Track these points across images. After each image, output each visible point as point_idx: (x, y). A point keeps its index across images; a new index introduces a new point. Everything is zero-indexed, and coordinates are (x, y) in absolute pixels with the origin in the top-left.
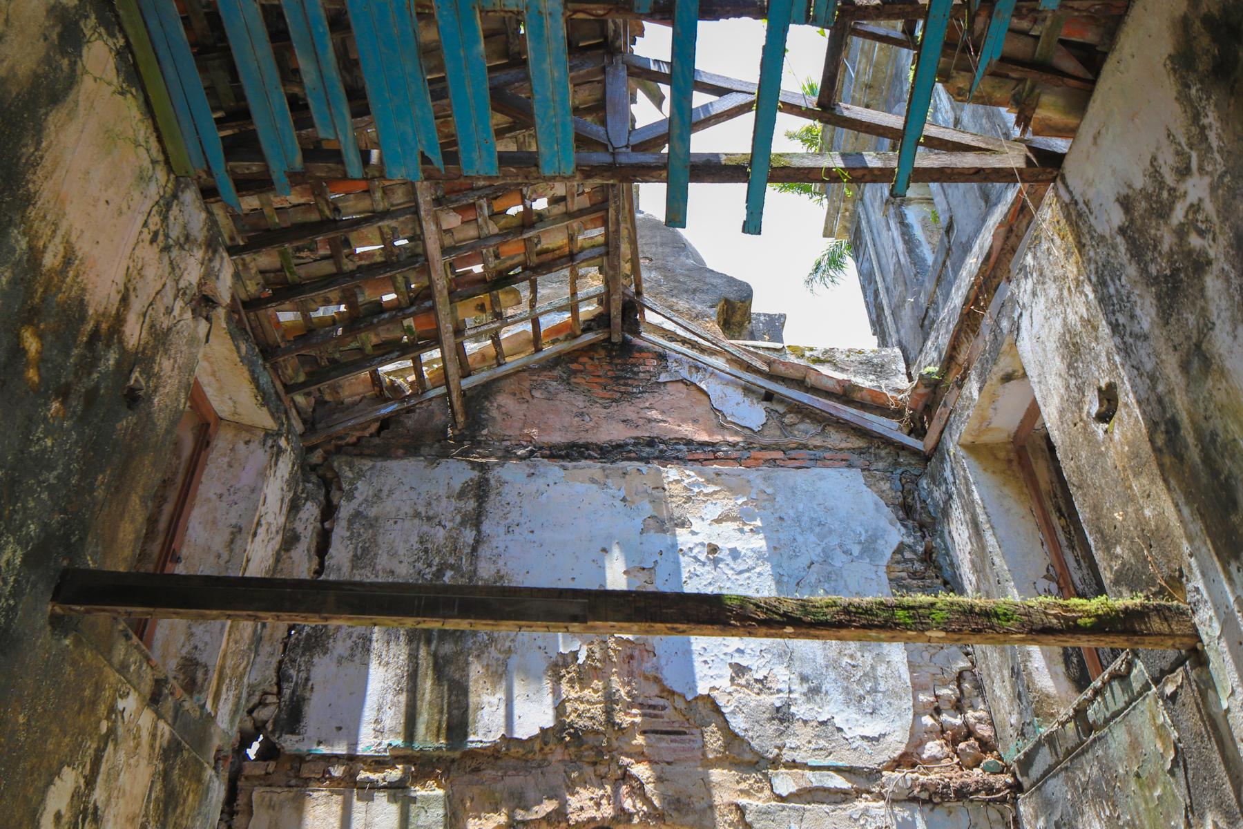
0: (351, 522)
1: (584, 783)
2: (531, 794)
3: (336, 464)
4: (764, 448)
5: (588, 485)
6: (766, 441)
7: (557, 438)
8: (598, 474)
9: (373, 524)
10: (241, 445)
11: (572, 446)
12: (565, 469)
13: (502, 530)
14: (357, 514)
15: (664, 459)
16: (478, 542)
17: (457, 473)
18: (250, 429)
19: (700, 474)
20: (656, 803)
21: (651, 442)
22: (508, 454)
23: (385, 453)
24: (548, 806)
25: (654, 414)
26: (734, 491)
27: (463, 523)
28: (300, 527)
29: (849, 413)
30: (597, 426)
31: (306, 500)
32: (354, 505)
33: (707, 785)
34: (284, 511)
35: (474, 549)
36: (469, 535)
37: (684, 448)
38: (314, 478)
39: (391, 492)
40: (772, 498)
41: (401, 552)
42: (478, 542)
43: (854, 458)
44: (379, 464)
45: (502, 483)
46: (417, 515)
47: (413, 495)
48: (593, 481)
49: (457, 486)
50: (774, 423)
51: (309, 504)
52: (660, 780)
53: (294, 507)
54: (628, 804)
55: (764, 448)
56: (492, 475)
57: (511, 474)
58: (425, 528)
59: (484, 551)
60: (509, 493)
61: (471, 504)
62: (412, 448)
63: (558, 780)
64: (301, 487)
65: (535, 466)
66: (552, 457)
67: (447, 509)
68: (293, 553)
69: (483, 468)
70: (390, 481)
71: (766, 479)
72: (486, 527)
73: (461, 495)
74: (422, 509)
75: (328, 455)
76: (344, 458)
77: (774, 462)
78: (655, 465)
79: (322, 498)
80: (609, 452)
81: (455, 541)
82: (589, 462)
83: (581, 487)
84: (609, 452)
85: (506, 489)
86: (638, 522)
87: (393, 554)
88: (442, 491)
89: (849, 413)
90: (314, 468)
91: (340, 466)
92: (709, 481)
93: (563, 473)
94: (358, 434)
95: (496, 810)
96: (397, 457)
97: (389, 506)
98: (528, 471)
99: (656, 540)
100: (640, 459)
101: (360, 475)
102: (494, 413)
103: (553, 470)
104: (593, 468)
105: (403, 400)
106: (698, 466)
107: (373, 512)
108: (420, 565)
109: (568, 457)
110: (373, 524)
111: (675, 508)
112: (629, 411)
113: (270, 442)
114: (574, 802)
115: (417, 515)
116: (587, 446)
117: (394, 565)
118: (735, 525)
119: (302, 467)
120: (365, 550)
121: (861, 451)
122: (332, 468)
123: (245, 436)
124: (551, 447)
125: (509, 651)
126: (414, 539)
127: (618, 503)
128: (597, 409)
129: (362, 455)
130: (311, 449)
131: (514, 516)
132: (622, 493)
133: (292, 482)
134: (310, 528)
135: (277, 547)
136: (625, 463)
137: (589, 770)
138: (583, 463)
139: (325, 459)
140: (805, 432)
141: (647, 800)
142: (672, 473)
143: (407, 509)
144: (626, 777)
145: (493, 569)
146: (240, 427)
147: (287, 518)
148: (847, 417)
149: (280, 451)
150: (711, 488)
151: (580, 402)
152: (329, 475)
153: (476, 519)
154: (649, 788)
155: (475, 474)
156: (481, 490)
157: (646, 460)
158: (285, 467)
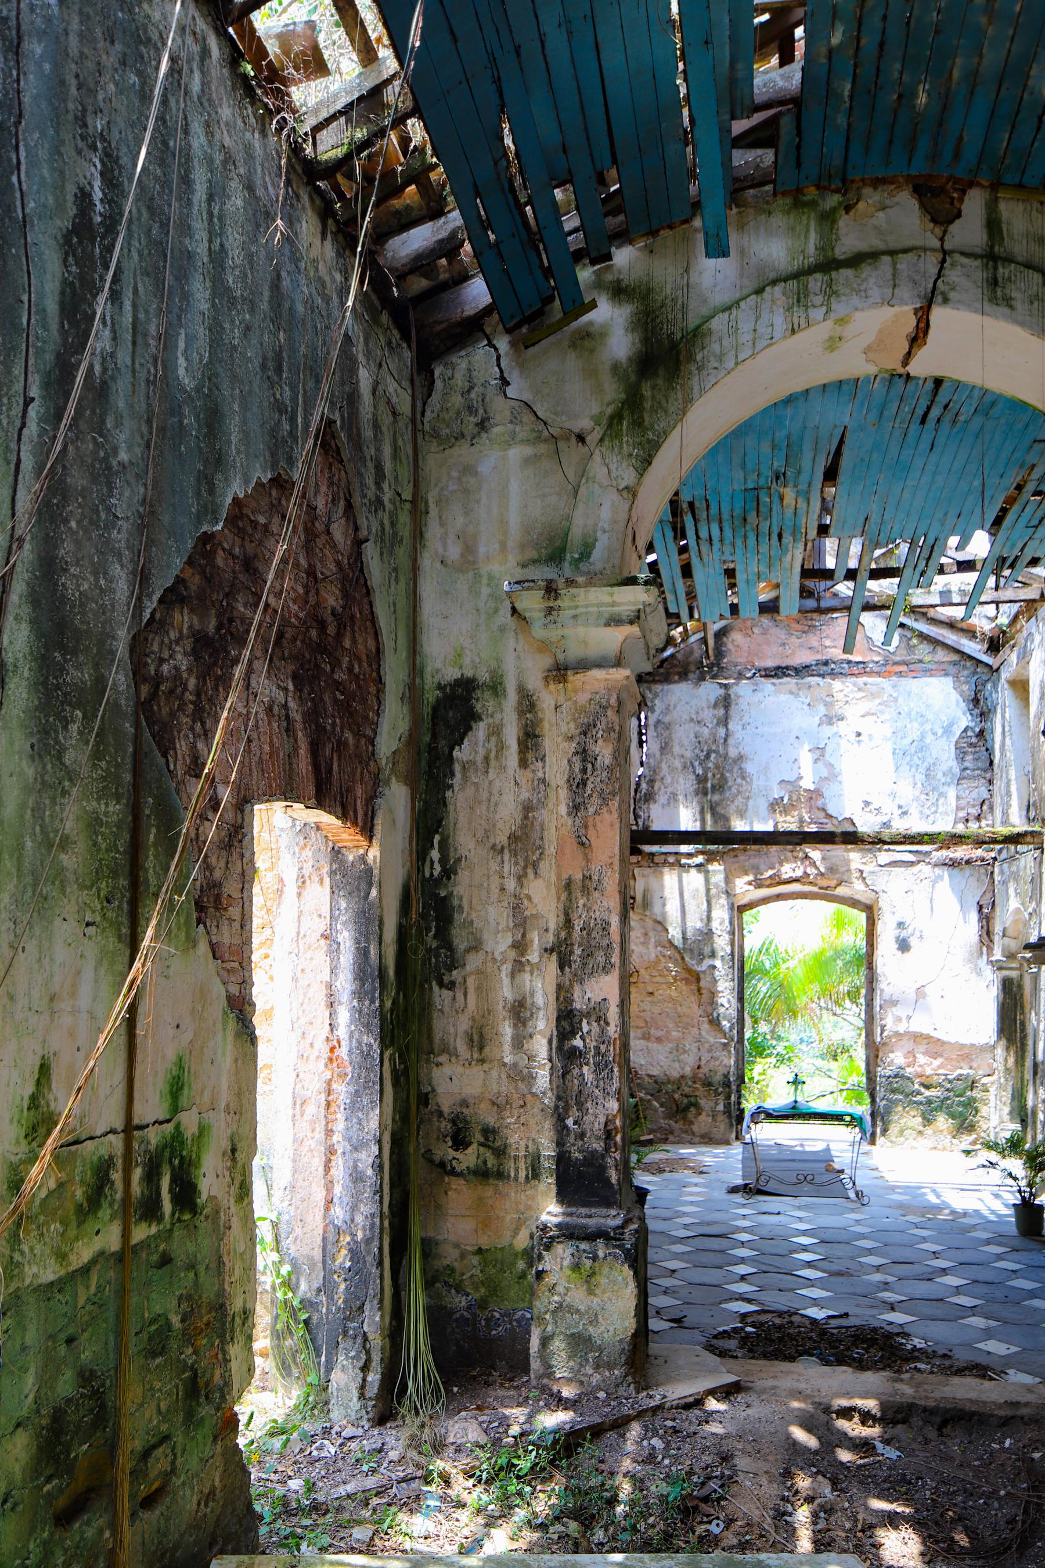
0: (656, 727)
1: (787, 861)
2: (762, 867)
4: (896, 663)
5: (788, 696)
6: (898, 659)
7: (770, 663)
8: (794, 688)
9: (668, 727)
11: (778, 668)
12: (774, 684)
13: (740, 727)
14: (658, 722)
15: (833, 675)
16: (727, 735)
17: (710, 690)
19: (854, 685)
20: (822, 870)
21: (826, 663)
22: (740, 676)
23: (667, 679)
24: (770, 872)
25: (827, 643)
26: (873, 696)
27: (718, 724)
29: (951, 637)
30: (793, 654)
32: (656, 714)
33: (848, 862)
35: (726, 740)
36: (722, 732)
37: (845, 666)
39: (675, 706)
40: (896, 700)
41: (686, 743)
42: (727, 735)
43: (952, 669)
44: (666, 687)
45: (738, 697)
46: (692, 720)
47: (688, 707)
48: (791, 693)
49: (713, 701)
50: (903, 645)
52: (823, 859)
54: (809, 870)
55: (896, 663)
56: (731, 692)
57: (743, 689)
58: (697, 728)
59: (731, 741)
60: (743, 703)
61: (722, 711)
62: (684, 676)
63: (775, 860)
65: (756, 684)
66: (766, 676)
67: (709, 715)
69: (726, 686)
70: (672, 699)
71: (894, 687)
72: (730, 726)
73: (715, 706)
74: (694, 717)
77: (900, 674)
78: (828, 680)
80: (801, 671)
81: (715, 735)
82: (788, 679)
83: (783, 697)
84: (801, 671)
85: (741, 700)
86: (817, 720)
87: (682, 745)
88: (704, 704)
89: (951, 637)
92: (860, 690)
93: (773, 688)
95: (746, 874)
96: (675, 682)
97: (675, 715)
98: (753, 688)
99: (827, 731)
100: (819, 675)
101: (656, 695)
102: (730, 646)
103: (768, 685)
104: (790, 682)
105: (675, 646)
106: (854, 679)
107: (666, 720)
108: (697, 751)
109: (775, 676)
110: (668, 727)
111: (838, 709)
112: (813, 640)
114: (783, 869)
115: (692, 720)
116: (787, 668)
117: (682, 751)
118: (874, 718)
120: (666, 744)
121: (955, 664)
124: (765, 670)
125: (748, 798)
126: (692, 736)
127: (806, 707)
128: (793, 639)
129: (654, 681)
131: (746, 719)
132: (808, 701)
136: (810, 679)
137: (789, 854)
138: (785, 680)
140: (923, 650)
141: (817, 868)
142: (837, 685)
143: (685, 717)
144: (807, 857)
145: (737, 752)
148: (949, 642)
150: (861, 694)
151: (781, 634)
153: (725, 721)
154: (818, 863)
155: (722, 691)
156: (726, 702)
157: (823, 676)
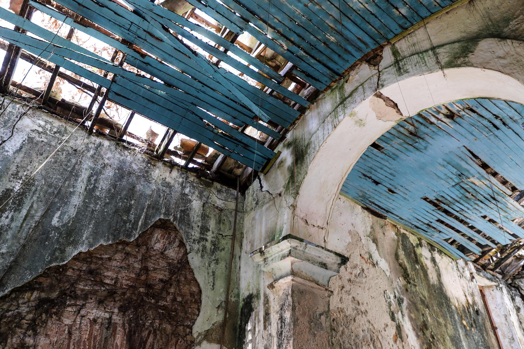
3: (516, 283)
10: (492, 292)
18: (491, 286)
28: (519, 305)
31: (515, 296)
34: (511, 302)
38: (513, 289)
51: (516, 297)
53: (513, 299)
64: (511, 293)
68: (521, 313)
75: (512, 280)
76: (518, 280)
79: (519, 294)
90: (510, 284)
91: (518, 283)
94: (517, 271)
113: (498, 288)
119: (508, 287)
122: (516, 284)
123: (491, 289)
130: (507, 280)
133: (509, 292)
134: (521, 304)
135: (516, 312)
139: (512, 281)
146: (489, 287)
147: (513, 303)
149: (501, 288)
152: (516, 286)
158: (505, 290)
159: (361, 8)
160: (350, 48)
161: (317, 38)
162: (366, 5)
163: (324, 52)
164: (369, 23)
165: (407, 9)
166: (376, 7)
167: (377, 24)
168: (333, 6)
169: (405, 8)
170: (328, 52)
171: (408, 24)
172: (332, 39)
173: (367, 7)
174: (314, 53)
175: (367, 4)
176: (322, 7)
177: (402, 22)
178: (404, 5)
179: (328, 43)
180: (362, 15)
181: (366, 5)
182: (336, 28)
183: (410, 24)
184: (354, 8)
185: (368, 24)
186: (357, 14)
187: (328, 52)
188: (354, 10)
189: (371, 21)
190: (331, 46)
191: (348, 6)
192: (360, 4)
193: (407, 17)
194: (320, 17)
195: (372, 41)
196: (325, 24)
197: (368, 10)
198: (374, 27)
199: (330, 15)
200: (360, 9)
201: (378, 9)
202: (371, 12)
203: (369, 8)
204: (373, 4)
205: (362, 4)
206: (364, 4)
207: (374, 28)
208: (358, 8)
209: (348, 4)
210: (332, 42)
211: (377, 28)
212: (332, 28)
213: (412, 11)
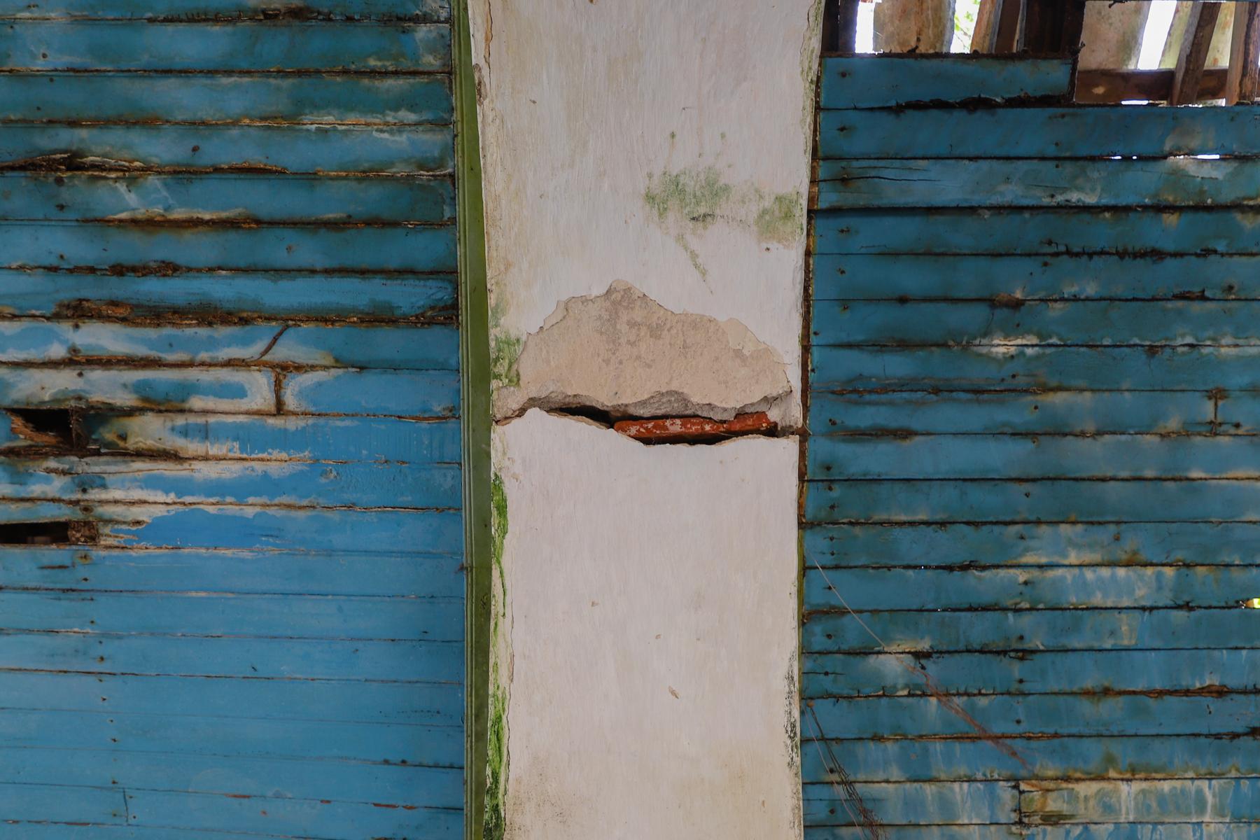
159: (1027, 550)
160: (896, 365)
161: (1063, 299)
162: (1022, 576)
163: (983, 263)
164: (943, 524)
165: (889, 682)
166: (986, 599)
167: (910, 545)
168: (1124, 474)
169: (901, 682)
170: (968, 277)
171: (819, 642)
172: (1001, 347)
173: (1012, 571)
174: (1032, 231)
175: (1026, 583)
176: (1156, 439)
177: (853, 629)
178: (917, 686)
179: (1002, 313)
180: (997, 529)
181: (1022, 576)
182: (1030, 398)
183: (816, 648)
184: (1044, 530)
185: (939, 517)
186: (1018, 518)
187: (968, 277)
188: (1038, 522)
189: (942, 536)
190: (981, 311)
191: (1073, 518)
192: (1044, 560)
193: (852, 659)
194: (1127, 395)
195: (855, 470)
196: (1081, 383)
197: (998, 567)
198: (909, 530)
199: (1099, 433)
200: (1023, 544)
201: (975, 600)
202: (984, 568)
203: (1002, 573)
204: (1009, 603)
205: (1040, 567)
206: (1036, 573)
207: (902, 524)
208: (1032, 543)
209: (1079, 528)
210: (986, 334)
211: (897, 531)
212: (1047, 389)
213: (866, 691)
